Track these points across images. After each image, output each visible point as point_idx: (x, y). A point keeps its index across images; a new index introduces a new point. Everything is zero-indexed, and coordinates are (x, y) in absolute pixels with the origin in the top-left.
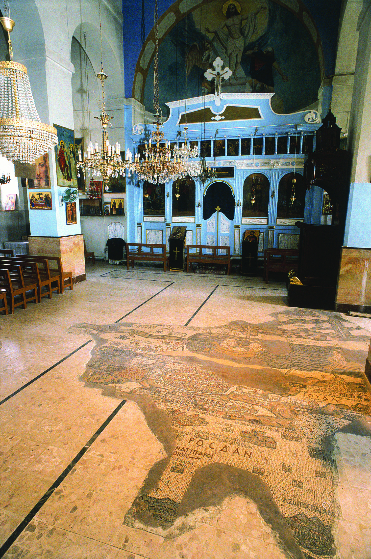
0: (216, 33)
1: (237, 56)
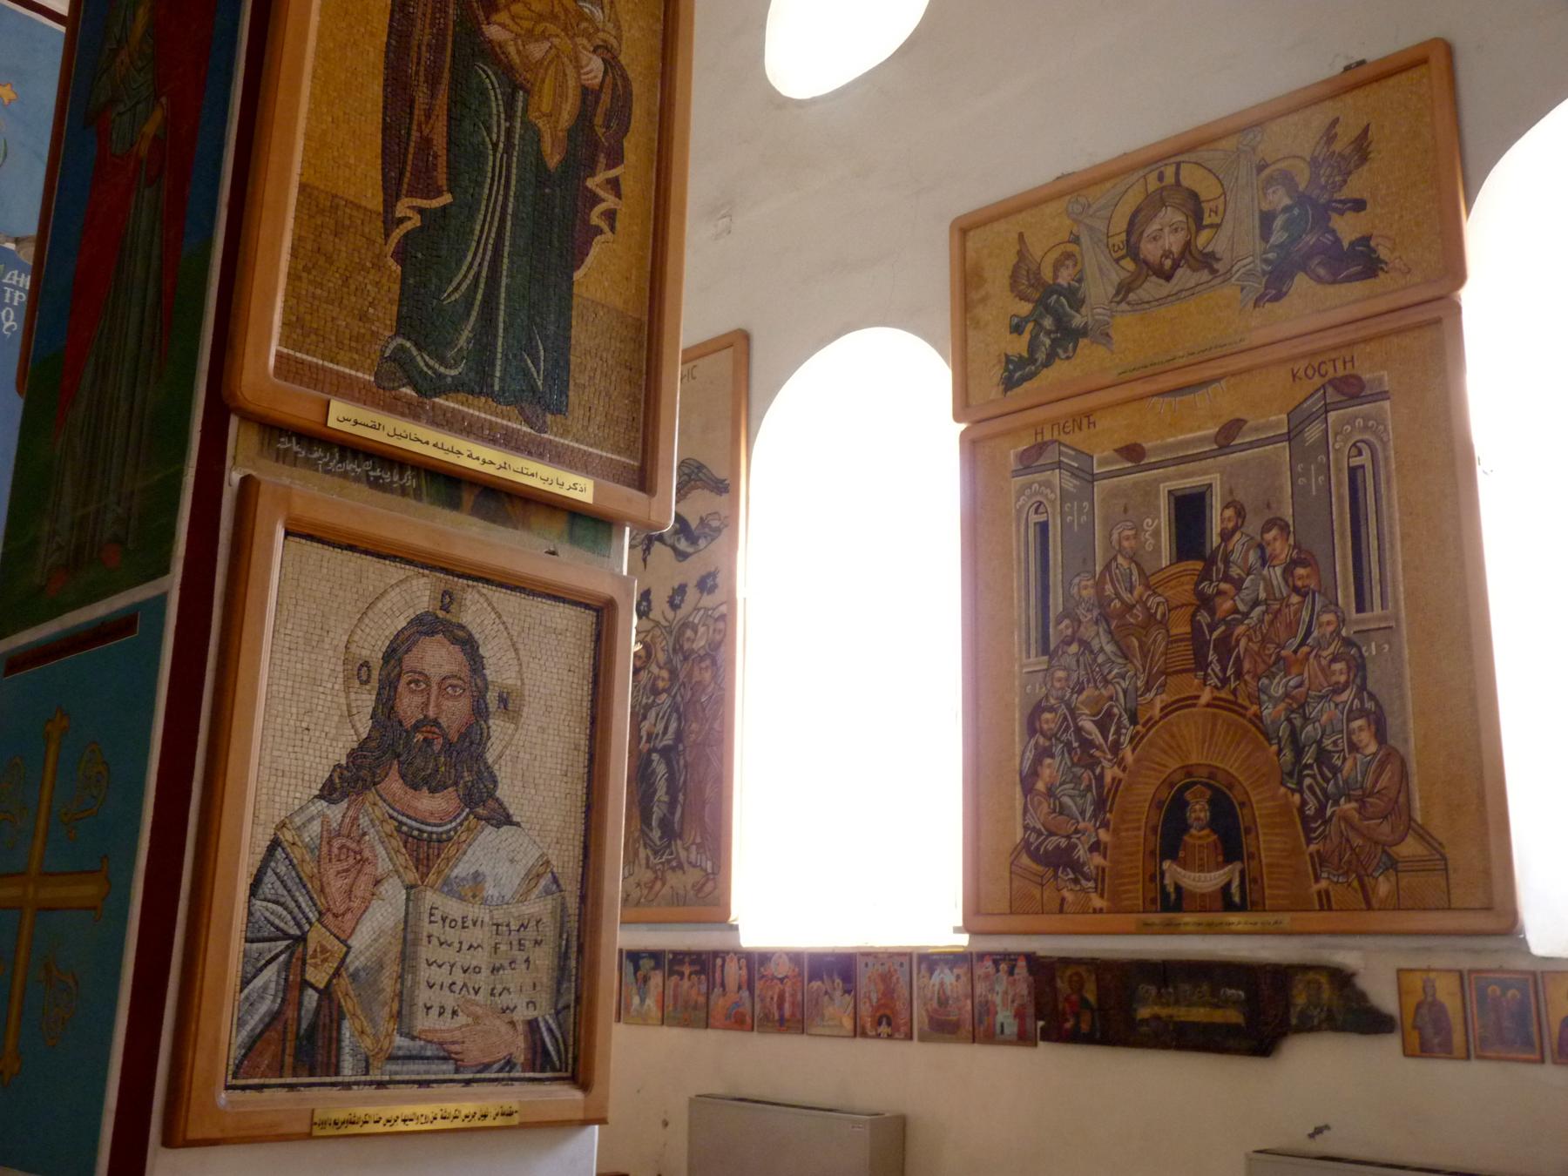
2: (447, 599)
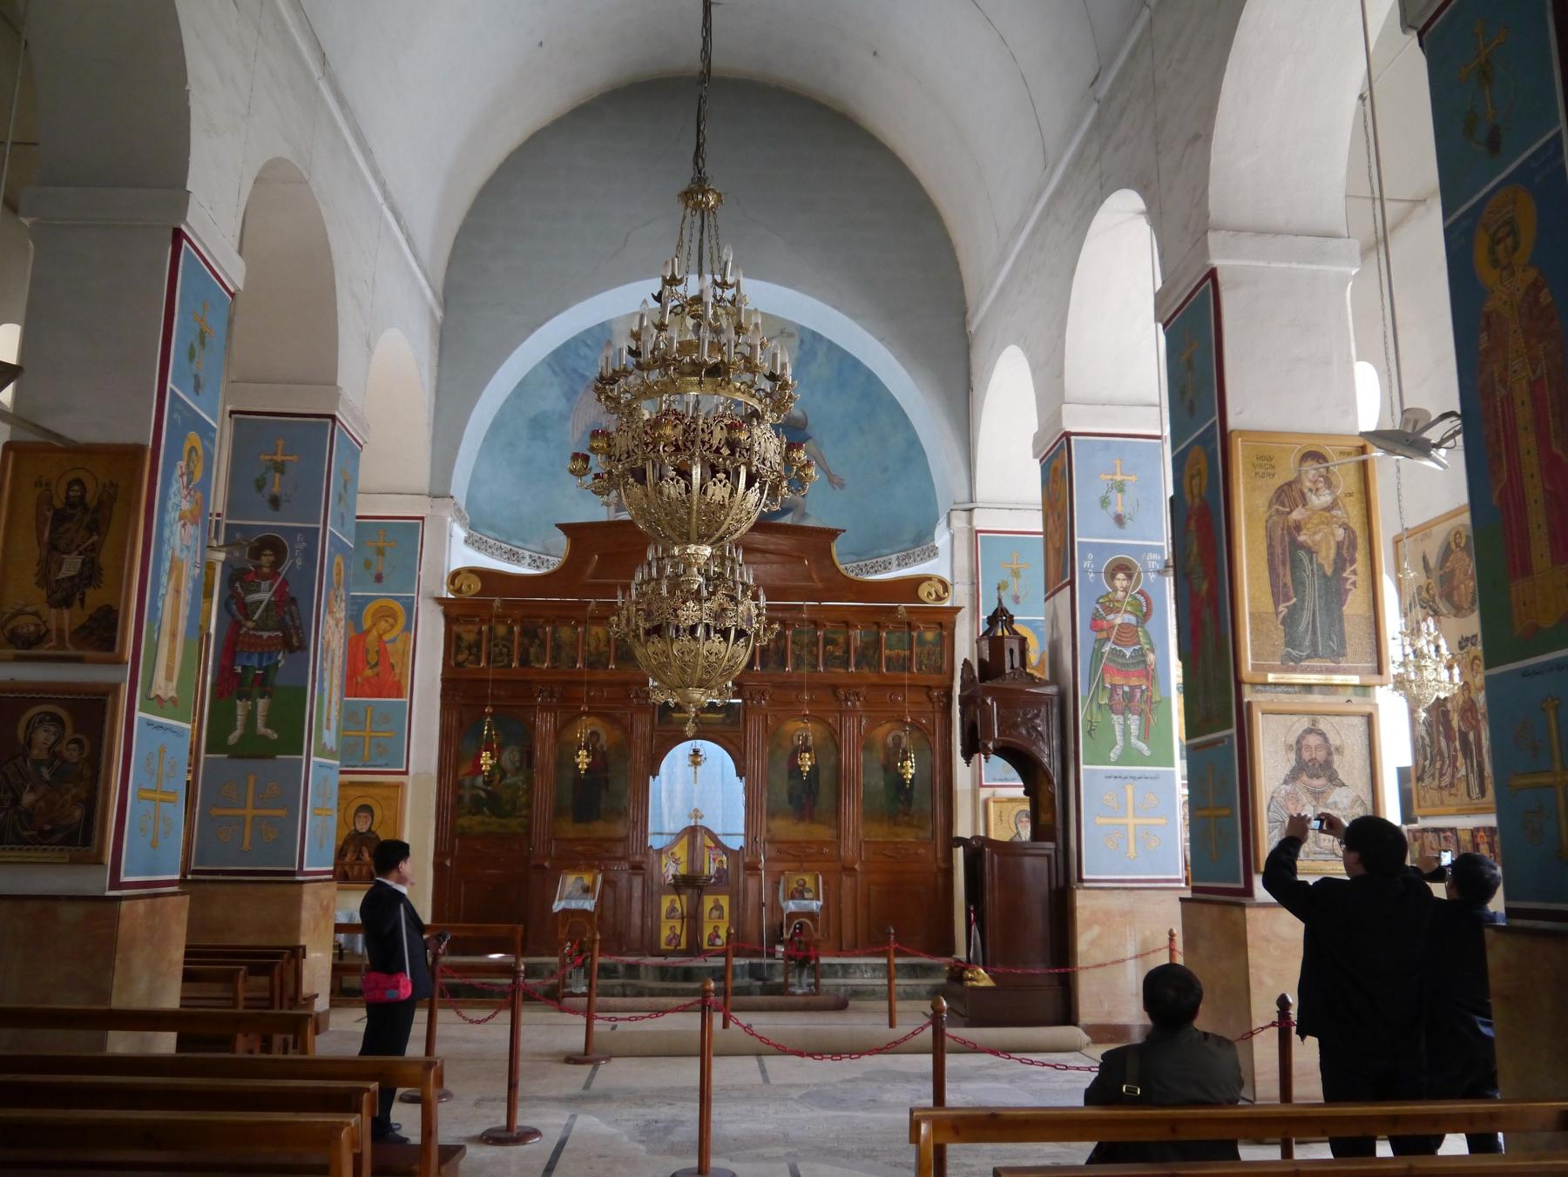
2: (1314, 722)
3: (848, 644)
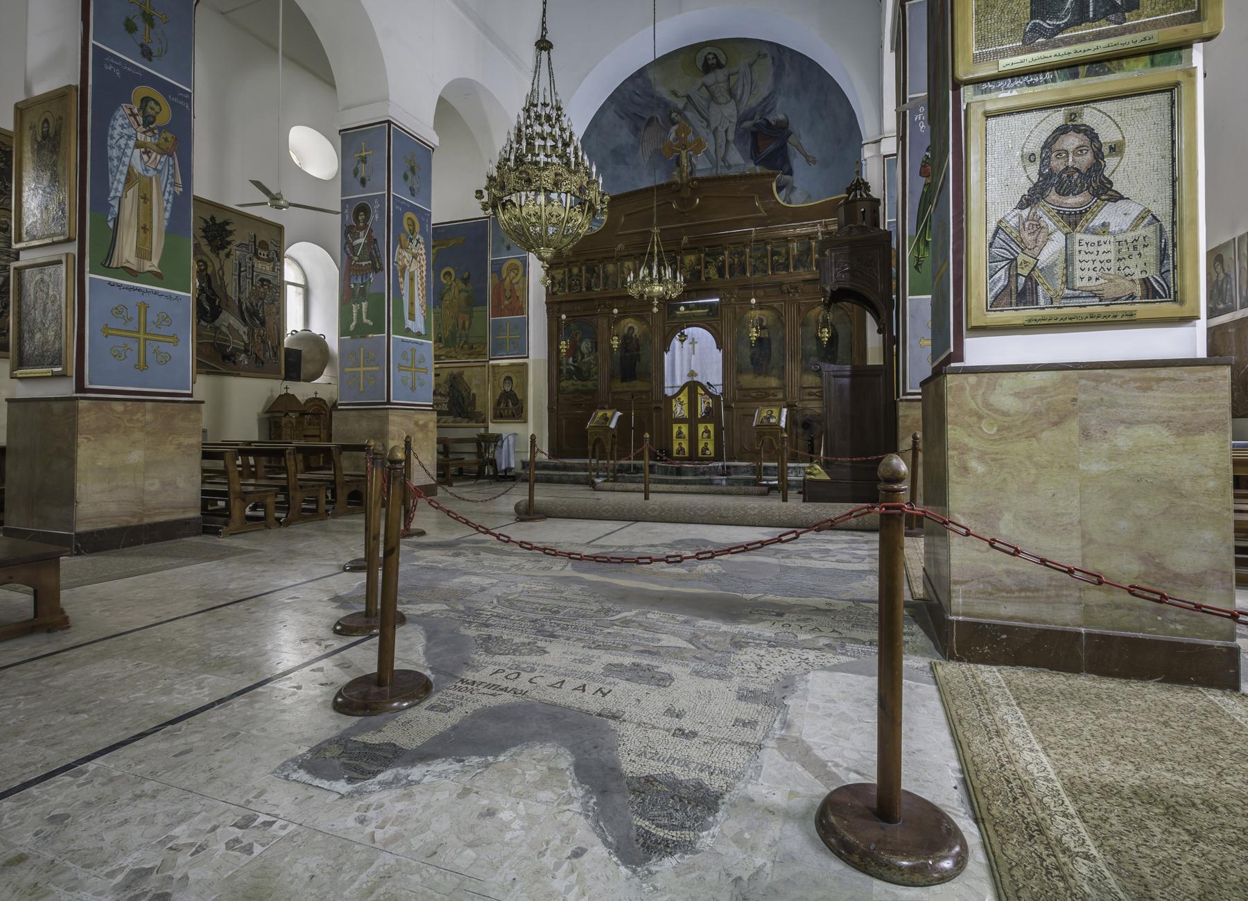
0: (688, 97)
1: (726, 131)
3: (788, 253)
